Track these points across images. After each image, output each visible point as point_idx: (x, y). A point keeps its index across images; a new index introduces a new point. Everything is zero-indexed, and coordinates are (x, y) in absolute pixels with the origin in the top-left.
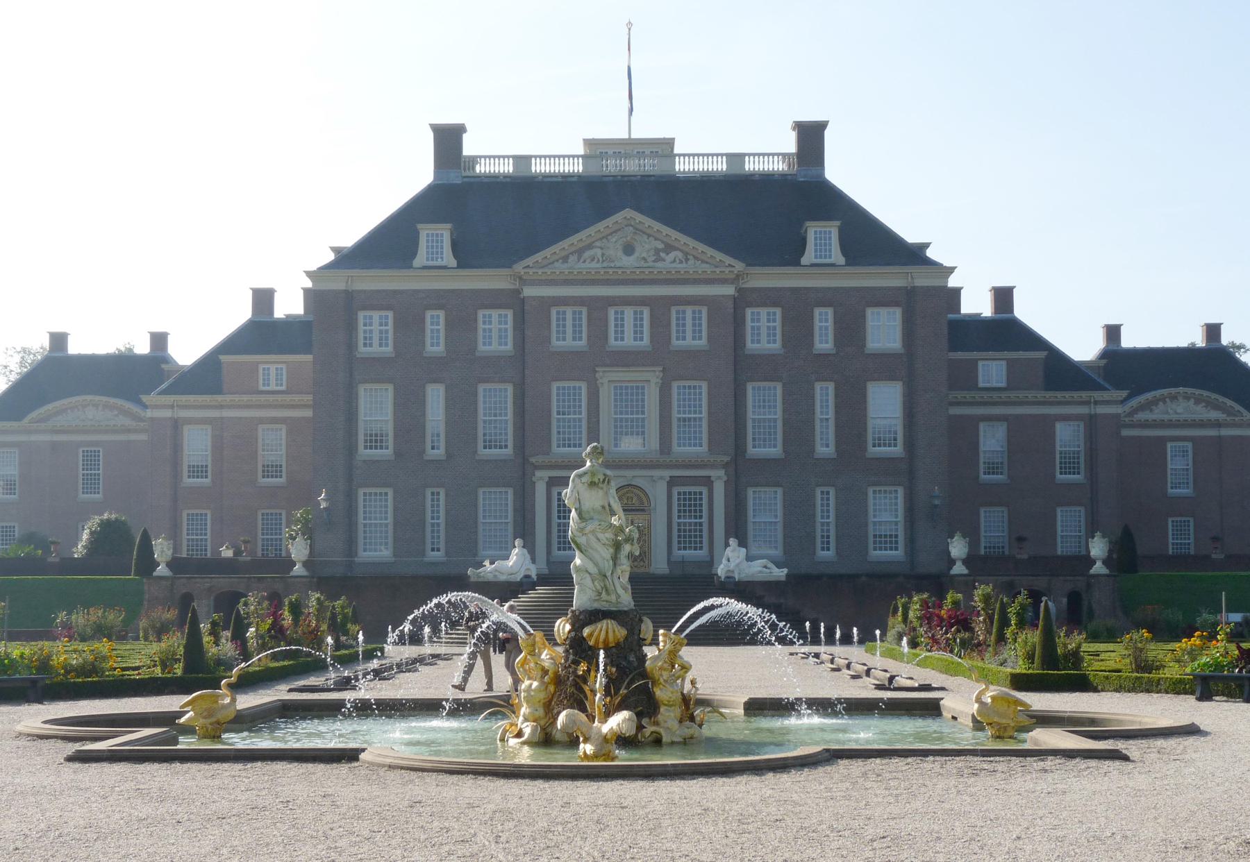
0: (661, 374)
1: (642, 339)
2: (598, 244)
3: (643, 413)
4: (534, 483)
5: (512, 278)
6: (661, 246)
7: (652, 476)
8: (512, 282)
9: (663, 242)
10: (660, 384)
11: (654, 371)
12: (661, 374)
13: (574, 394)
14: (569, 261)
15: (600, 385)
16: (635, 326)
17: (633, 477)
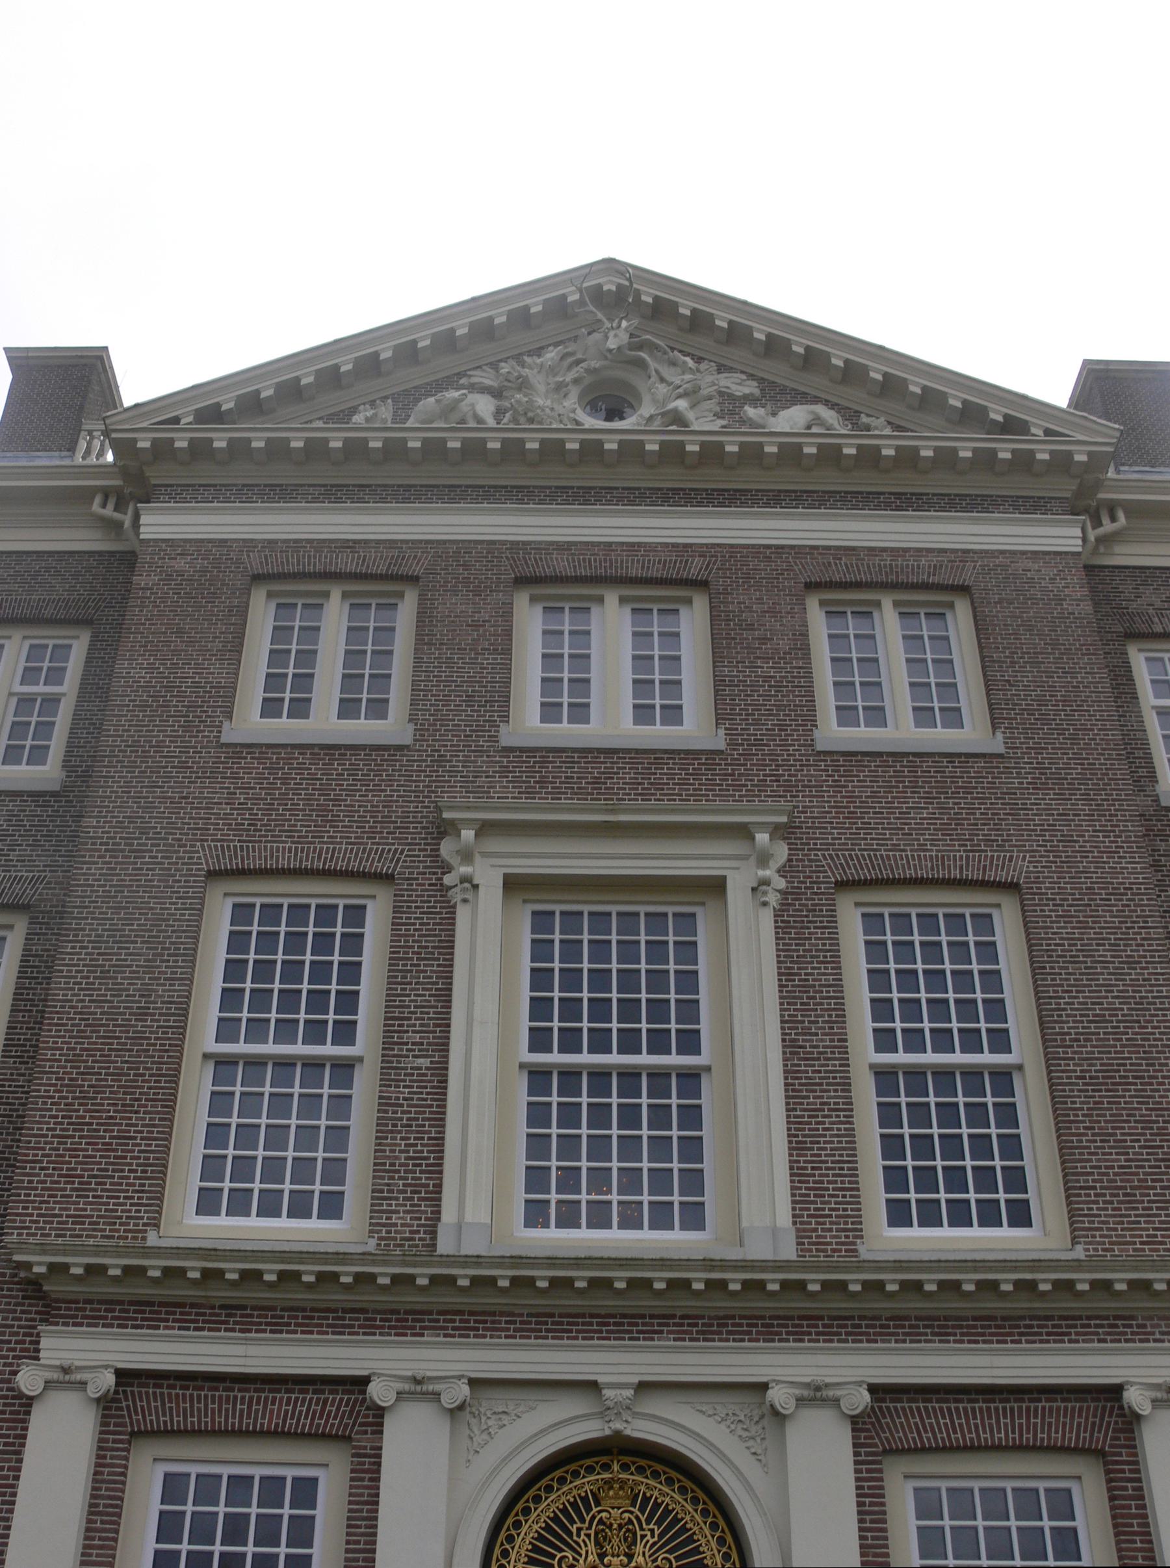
0: (782, 852)
1: (673, 714)
2: (486, 378)
3: (690, 1042)
4: (28, 1403)
5: (111, 505)
6: (750, 388)
7: (764, 1387)
8: (109, 511)
9: (751, 376)
10: (773, 899)
11: (744, 832)
12: (782, 852)
13: (323, 942)
14: (358, 419)
15: (456, 896)
16: (641, 661)
17: (643, 1387)
